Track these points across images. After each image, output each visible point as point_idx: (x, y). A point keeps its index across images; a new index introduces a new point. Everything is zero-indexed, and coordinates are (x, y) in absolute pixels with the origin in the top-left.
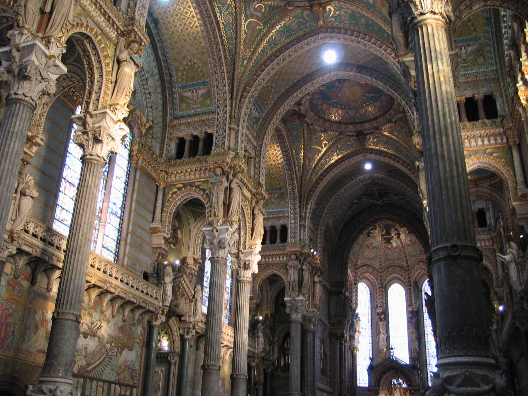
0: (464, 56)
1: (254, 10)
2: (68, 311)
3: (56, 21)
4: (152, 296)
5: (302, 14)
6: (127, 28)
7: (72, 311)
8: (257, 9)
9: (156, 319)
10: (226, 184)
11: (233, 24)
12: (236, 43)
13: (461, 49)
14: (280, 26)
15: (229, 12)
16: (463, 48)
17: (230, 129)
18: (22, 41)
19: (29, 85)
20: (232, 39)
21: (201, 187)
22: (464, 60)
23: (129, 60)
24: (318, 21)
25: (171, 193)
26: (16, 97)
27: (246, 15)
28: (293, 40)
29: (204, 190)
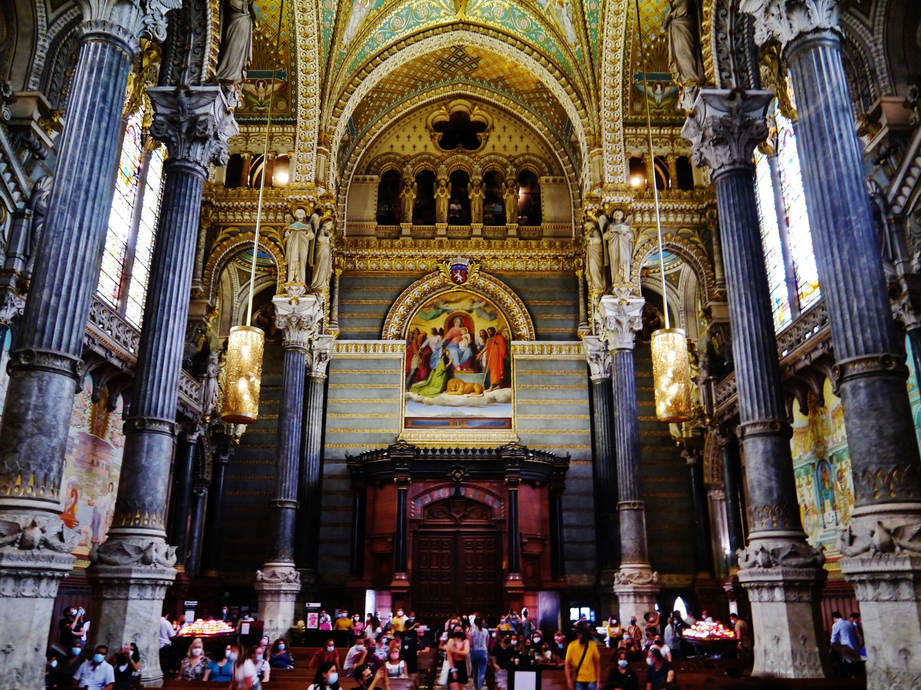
0: (658, 98)
2: (158, 417)
4: (191, 396)
7: (165, 419)
9: (193, 432)
10: (312, 235)
12: (336, 21)
13: (656, 88)
14: (402, 7)
16: (659, 87)
17: (318, 151)
20: (330, 13)
21: (270, 236)
22: (658, 105)
23: (246, 10)
25: (219, 239)
29: (275, 241)
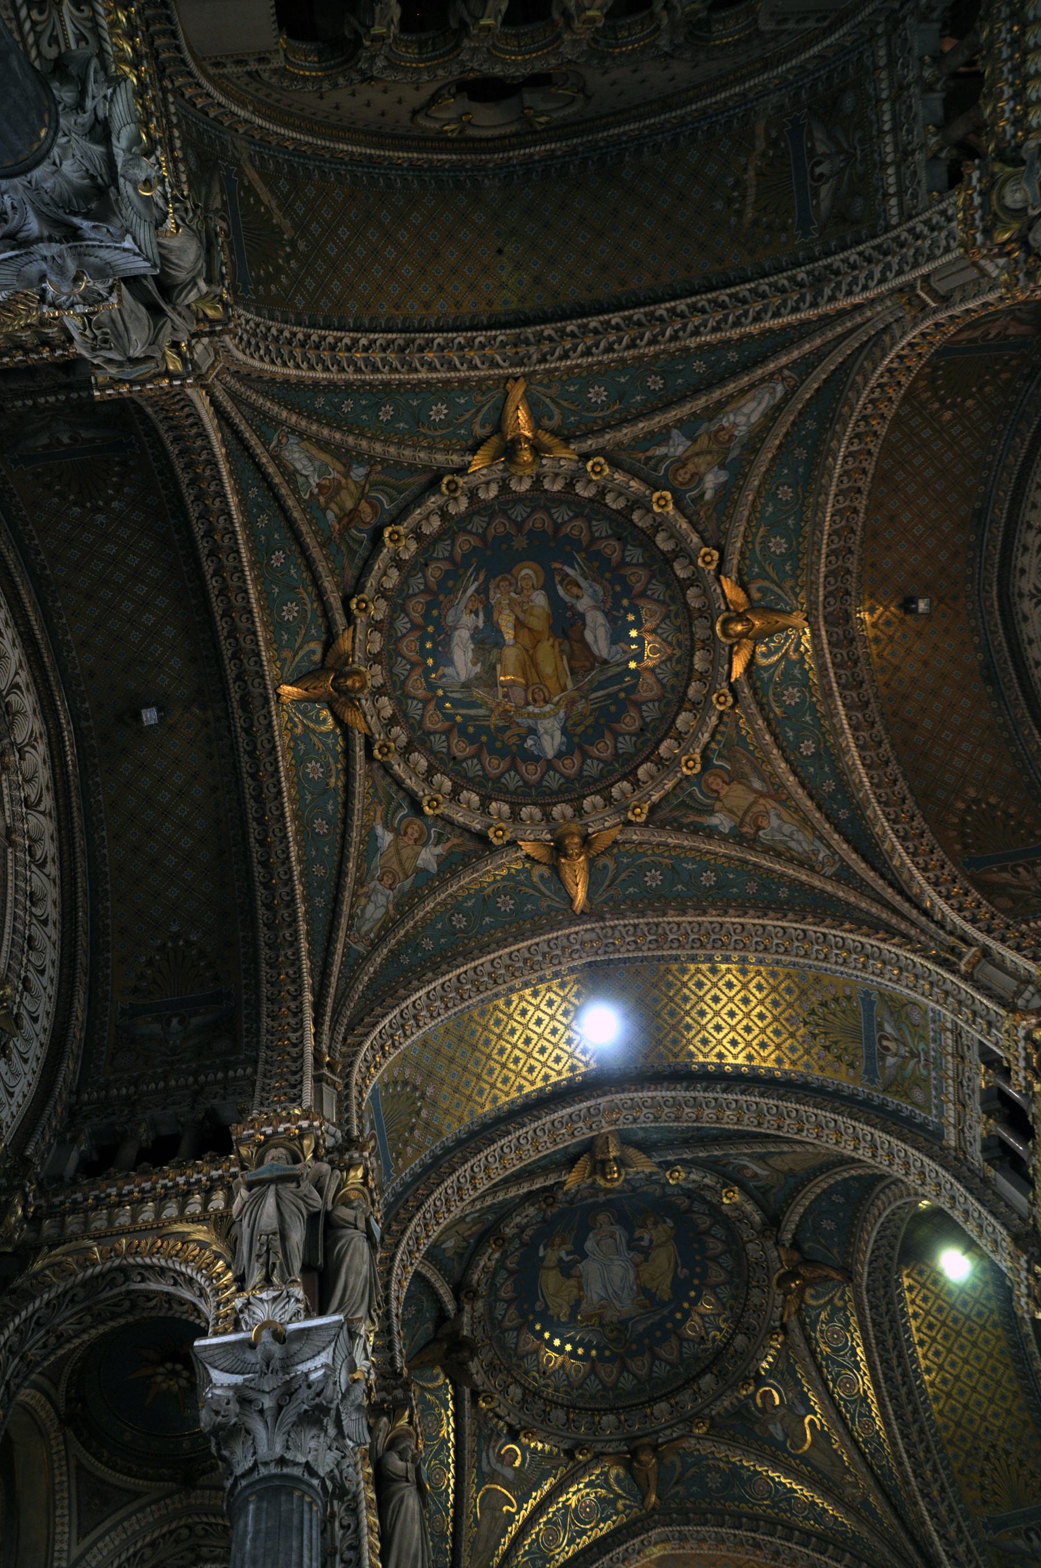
1: (498, 1461)
3: (353, 1289)
5: (606, 1474)
6: (389, 1394)
8: (503, 1456)
11: (448, 1495)
12: (456, 1551)
15: (442, 1462)
18: (286, 1317)
19: (312, 1444)
20: (443, 1536)
23: (412, 1476)
24: (645, 1497)
26: (285, 1470)
27: (481, 1474)
28: (588, 1548)
